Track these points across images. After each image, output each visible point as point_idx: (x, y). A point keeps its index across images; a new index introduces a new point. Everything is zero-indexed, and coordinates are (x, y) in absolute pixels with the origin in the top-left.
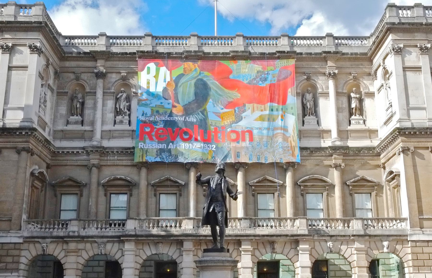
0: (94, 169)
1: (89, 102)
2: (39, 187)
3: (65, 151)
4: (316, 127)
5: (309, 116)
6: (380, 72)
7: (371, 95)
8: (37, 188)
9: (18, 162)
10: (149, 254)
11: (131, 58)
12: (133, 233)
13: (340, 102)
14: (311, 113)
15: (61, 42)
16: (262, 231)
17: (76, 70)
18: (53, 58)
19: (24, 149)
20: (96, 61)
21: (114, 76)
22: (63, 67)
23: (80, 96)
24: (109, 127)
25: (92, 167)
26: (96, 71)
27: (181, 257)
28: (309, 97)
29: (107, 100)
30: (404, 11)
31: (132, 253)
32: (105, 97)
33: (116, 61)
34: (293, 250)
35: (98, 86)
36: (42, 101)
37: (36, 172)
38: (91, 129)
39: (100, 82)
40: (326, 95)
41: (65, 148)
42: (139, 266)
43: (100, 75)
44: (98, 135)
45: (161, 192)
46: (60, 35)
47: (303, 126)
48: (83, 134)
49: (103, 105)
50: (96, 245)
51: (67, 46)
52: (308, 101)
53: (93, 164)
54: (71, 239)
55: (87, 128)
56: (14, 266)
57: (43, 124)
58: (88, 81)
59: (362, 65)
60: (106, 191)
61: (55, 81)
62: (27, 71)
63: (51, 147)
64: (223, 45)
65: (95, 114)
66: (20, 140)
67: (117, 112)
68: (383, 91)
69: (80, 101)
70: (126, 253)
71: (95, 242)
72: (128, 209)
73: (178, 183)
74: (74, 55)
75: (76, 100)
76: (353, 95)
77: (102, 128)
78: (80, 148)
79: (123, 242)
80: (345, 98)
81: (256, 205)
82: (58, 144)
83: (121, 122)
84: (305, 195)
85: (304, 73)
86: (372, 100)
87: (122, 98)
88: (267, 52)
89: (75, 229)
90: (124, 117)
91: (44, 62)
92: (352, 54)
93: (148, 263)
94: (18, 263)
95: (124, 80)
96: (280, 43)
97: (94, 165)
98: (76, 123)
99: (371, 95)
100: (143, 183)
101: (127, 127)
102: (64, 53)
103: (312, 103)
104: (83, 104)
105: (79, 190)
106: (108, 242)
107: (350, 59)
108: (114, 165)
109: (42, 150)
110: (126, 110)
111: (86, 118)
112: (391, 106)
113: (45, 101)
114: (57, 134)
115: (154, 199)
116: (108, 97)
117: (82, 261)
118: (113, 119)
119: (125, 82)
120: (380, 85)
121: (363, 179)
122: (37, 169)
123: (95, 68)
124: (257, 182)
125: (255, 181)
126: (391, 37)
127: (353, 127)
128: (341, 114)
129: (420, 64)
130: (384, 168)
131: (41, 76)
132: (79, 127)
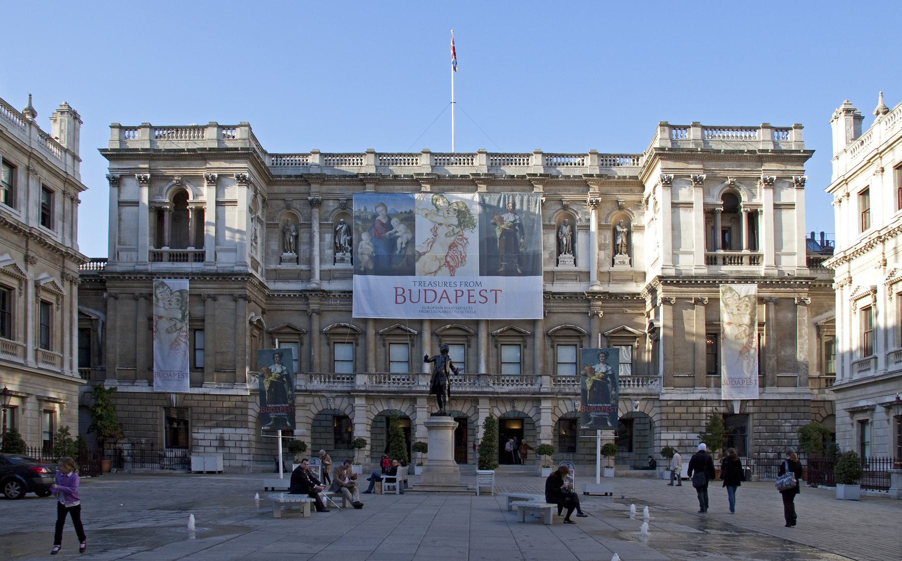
0: (315, 316)
1: (304, 237)
2: (257, 335)
3: (281, 294)
4: (573, 268)
5: (565, 254)
7: (641, 228)
8: (255, 337)
10: (381, 410)
11: (350, 181)
12: (363, 389)
13: (603, 237)
15: (268, 161)
16: (501, 388)
17: (289, 197)
18: (261, 185)
19: (241, 296)
20: (309, 185)
21: (331, 203)
22: (272, 194)
23: (292, 228)
24: (328, 266)
25: (312, 312)
27: (414, 413)
28: (566, 230)
29: (325, 233)
31: (364, 408)
32: (323, 229)
33: (333, 185)
34: (535, 408)
35: (313, 218)
36: (253, 238)
37: (255, 320)
38: (308, 269)
39: (316, 211)
41: (280, 291)
42: (370, 422)
43: (315, 204)
46: (265, 153)
47: (557, 266)
48: (299, 274)
49: (321, 239)
50: (324, 399)
52: (565, 235)
55: (303, 267)
56: (243, 418)
57: (255, 264)
58: (301, 210)
59: (631, 190)
61: (263, 211)
62: (237, 207)
64: (462, 164)
65: (311, 251)
66: (236, 286)
67: (337, 247)
69: (294, 234)
72: (354, 361)
73: (410, 332)
74: (283, 179)
76: (619, 229)
77: (320, 267)
78: (297, 291)
79: (353, 397)
80: (609, 232)
81: (499, 358)
82: (272, 286)
83: (342, 260)
84: (555, 348)
89: (302, 383)
90: (345, 254)
91: (252, 193)
93: (379, 419)
94: (247, 415)
95: (343, 209)
96: (532, 162)
97: (313, 311)
98: (290, 260)
99: (641, 228)
102: (272, 176)
103: (569, 238)
104: (297, 237)
105: (299, 339)
106: (337, 396)
107: (616, 183)
109: (257, 295)
110: (347, 246)
111: (301, 255)
113: (256, 237)
114: (268, 273)
115: (383, 349)
116: (326, 230)
117: (312, 416)
118: (333, 256)
119: (344, 211)
122: (255, 316)
123: (309, 194)
124: (501, 332)
125: (499, 331)
127: (617, 268)
129: (693, 199)
131: (251, 210)
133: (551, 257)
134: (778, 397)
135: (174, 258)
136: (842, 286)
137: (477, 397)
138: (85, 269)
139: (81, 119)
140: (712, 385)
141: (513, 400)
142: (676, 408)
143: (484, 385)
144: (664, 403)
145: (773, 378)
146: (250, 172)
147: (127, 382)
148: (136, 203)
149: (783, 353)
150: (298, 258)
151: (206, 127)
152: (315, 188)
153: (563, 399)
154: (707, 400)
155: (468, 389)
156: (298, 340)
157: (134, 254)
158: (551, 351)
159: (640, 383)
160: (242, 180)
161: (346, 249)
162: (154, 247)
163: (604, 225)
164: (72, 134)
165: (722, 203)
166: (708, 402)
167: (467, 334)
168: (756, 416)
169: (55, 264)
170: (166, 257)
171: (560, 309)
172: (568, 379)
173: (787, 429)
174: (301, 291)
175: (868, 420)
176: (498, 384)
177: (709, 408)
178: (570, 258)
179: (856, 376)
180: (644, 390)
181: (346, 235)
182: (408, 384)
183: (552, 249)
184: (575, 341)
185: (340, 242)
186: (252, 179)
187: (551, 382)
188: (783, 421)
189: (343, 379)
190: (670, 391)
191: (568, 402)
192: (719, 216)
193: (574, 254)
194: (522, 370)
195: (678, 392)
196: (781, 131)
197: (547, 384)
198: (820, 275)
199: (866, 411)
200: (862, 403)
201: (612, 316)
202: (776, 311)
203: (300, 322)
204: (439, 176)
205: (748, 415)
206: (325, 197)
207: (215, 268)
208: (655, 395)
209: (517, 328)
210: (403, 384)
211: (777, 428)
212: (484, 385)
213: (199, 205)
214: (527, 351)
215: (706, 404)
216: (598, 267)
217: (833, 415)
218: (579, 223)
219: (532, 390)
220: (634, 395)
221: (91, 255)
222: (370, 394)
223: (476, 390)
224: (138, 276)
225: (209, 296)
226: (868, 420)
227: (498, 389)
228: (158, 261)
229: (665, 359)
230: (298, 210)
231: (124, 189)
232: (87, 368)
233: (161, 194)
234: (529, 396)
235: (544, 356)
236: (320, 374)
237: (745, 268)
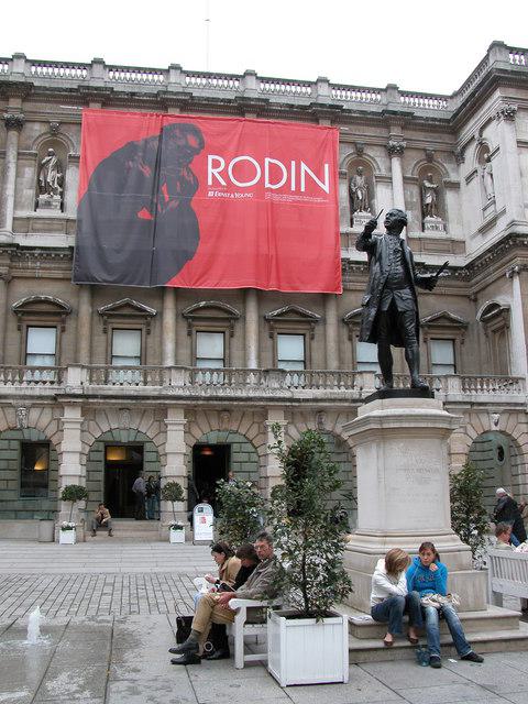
6: (471, 152)
7: (455, 186)
10: (105, 428)
12: (80, 392)
21: (37, 127)
26: (6, 115)
27: (162, 436)
29: (25, 166)
39: (13, 134)
40: (388, 180)
45: (116, 326)
50: (11, 410)
60: (20, 320)
68: (476, 181)
70: (66, 426)
73: (145, 311)
76: (427, 184)
79: (62, 407)
83: (48, 204)
85: (355, 143)
86: (457, 192)
99: (455, 186)
101: (56, 213)
106: (34, 406)
108: (34, 278)
112: (494, 202)
115: (103, 337)
120: (471, 170)
121: (444, 317)
124: (278, 315)
126: (498, 93)
127: (428, 234)
130: (475, 300)
137: (263, 407)
141: (320, 412)
155: (251, 394)
158: (347, 345)
161: (55, 190)
167: (226, 316)
204: (192, 98)
206: (32, 117)
208: (522, 404)
209: (301, 309)
214: (315, 344)
218: (377, 173)
220: (493, 404)
222: (91, 400)
223: (264, 395)
234: (346, 404)
235: (340, 351)
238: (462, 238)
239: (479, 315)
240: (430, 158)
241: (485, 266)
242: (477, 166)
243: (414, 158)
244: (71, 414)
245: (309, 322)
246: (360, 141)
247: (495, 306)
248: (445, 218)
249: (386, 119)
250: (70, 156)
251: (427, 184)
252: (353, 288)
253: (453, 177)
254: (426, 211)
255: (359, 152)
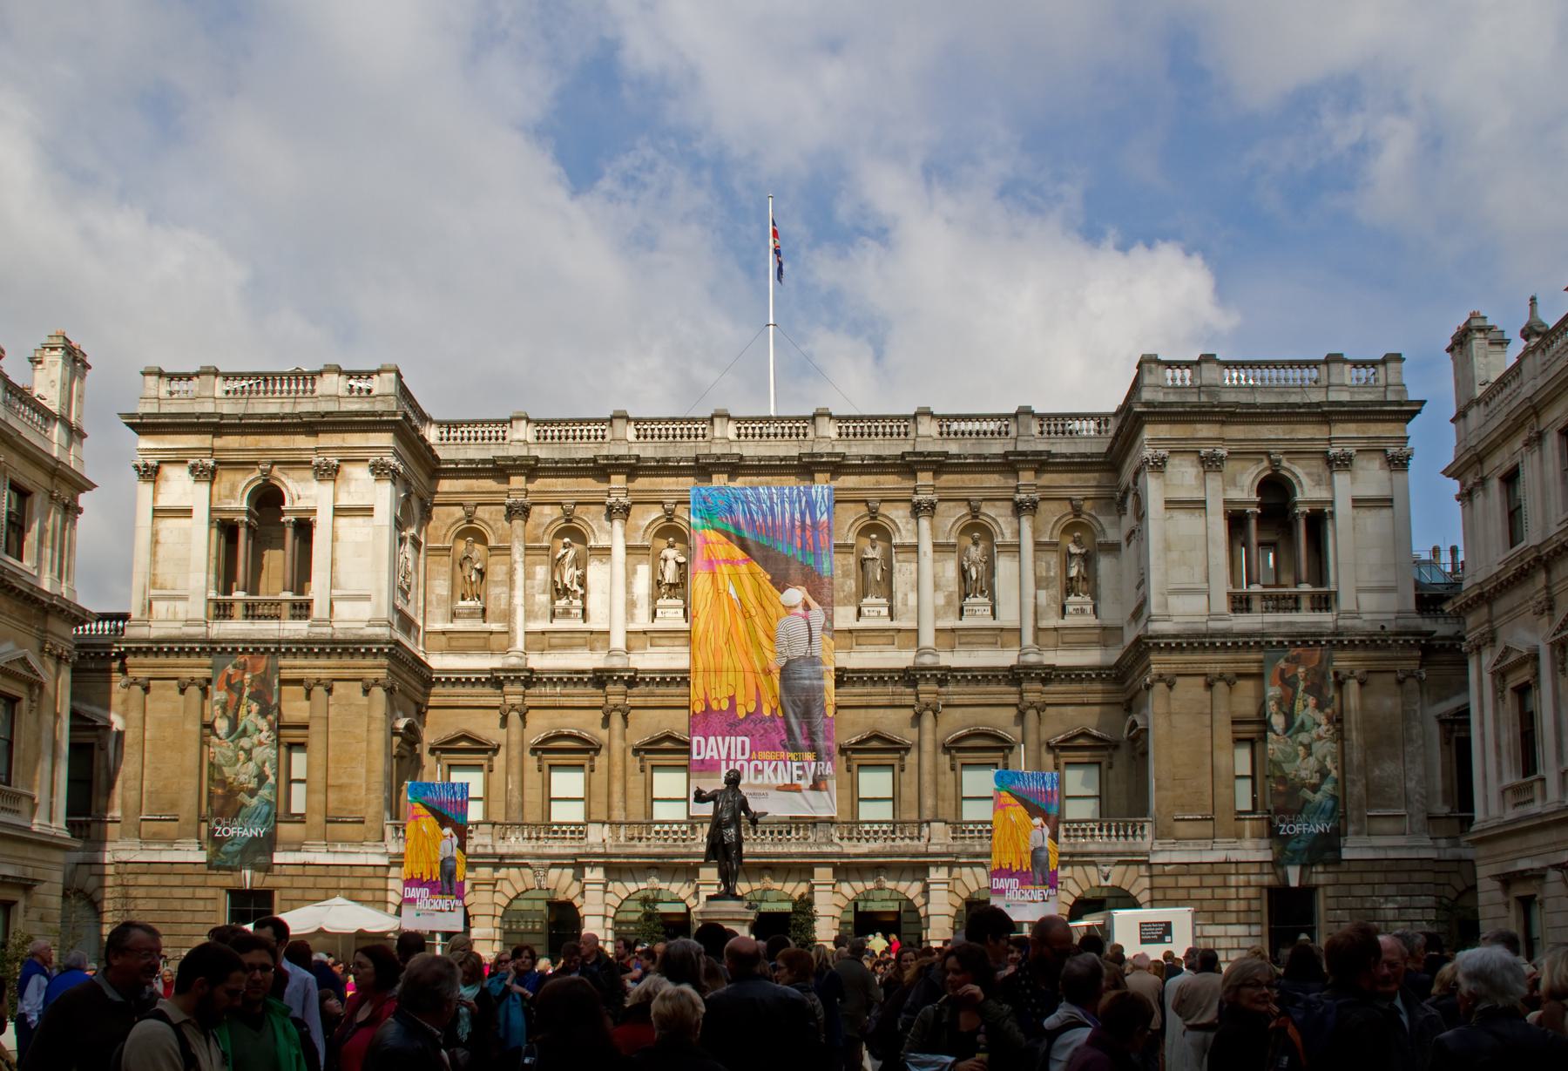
1: (497, 570)
4: (990, 623)
7: (1113, 548)
9: (369, 707)
12: (601, 850)
13: (1044, 564)
14: (978, 590)
19: (376, 682)
21: (547, 509)
26: (508, 501)
28: (976, 553)
29: (535, 564)
30: (1178, 372)
38: (505, 629)
40: (1015, 549)
44: (520, 644)
49: (528, 576)
51: (443, 445)
53: (513, 706)
54: (481, 860)
55: (495, 627)
58: (491, 523)
63: (424, 670)
65: (511, 597)
67: (557, 590)
69: (478, 566)
71: (526, 865)
72: (587, 799)
75: (468, 565)
80: (1055, 555)
81: (855, 789)
83: (566, 613)
86: (1114, 560)
87: (568, 559)
88: (885, 452)
89: (487, 840)
92: (1072, 455)
98: (471, 614)
99: (1113, 548)
100: (617, 744)
101: (578, 624)
103: (982, 567)
104: (482, 573)
106: (553, 866)
109: (409, 679)
110: (576, 587)
111: (491, 608)
117: (505, 902)
118: (549, 606)
127: (1069, 621)
128: (1042, 594)
132: (476, 625)
133: (949, 603)
134: (1370, 855)
135: (251, 612)
136: (1478, 648)
138: (87, 632)
139: (88, 361)
140: (1248, 833)
142: (1180, 878)
143: (824, 840)
144: (1156, 870)
145: (1360, 820)
146: (396, 453)
147: (159, 843)
148: (186, 512)
149: (1377, 772)
150: (484, 610)
151: (321, 373)
152: (517, 482)
153: (971, 865)
154: (1237, 863)
156: (483, 762)
157: (180, 605)
158: (950, 775)
159: (1113, 833)
160: (379, 470)
162: (217, 589)
163: (1046, 544)
164: (67, 387)
165: (1258, 499)
166: (1240, 866)
168: (1330, 891)
169: (29, 625)
170: (239, 609)
171: (966, 700)
172: (980, 827)
173: (1390, 914)
174: (493, 670)
175: (1535, 896)
176: (850, 839)
177: (1242, 877)
178: (984, 605)
179: (1511, 814)
180: (1120, 845)
181: (574, 568)
182: (684, 840)
183: (951, 589)
184: (996, 757)
185: (562, 581)
186: (401, 469)
187: (946, 834)
188: (1382, 900)
189: (564, 832)
190: (1168, 847)
191: (978, 870)
192: (1253, 523)
193: (992, 597)
194: (897, 813)
195: (1183, 848)
196: (1364, 366)
197: (939, 837)
198: (1442, 628)
199: (1532, 877)
200: (1523, 865)
201: (1063, 709)
202: (1362, 697)
203: (486, 726)
205: (1315, 888)
207: (328, 630)
208: (1142, 854)
210: (675, 840)
211: (1371, 913)
212: (824, 840)
213: (304, 516)
214: (905, 777)
215: (1237, 870)
216: (1036, 620)
217: (1474, 887)
219: (912, 850)
220: (1102, 854)
221: (95, 608)
224: (187, 645)
225: (318, 682)
226: (1535, 896)
227: (849, 847)
228: (224, 617)
229: (1158, 788)
230: (486, 523)
231: (163, 486)
232: (84, 819)
233: (232, 495)
236: (520, 825)
237: (1305, 618)
238: (1118, 623)
239: (1126, 732)
240: (1077, 511)
241: (1131, 667)
242: (1134, 523)
243: (1052, 514)
244: (595, 875)
245: (897, 751)
246: (974, 495)
247: (1134, 724)
248: (1095, 597)
249: (1010, 464)
250: (590, 549)
251: (1074, 549)
252: (957, 702)
253: (1112, 535)
254: (1070, 588)
255: (975, 512)
